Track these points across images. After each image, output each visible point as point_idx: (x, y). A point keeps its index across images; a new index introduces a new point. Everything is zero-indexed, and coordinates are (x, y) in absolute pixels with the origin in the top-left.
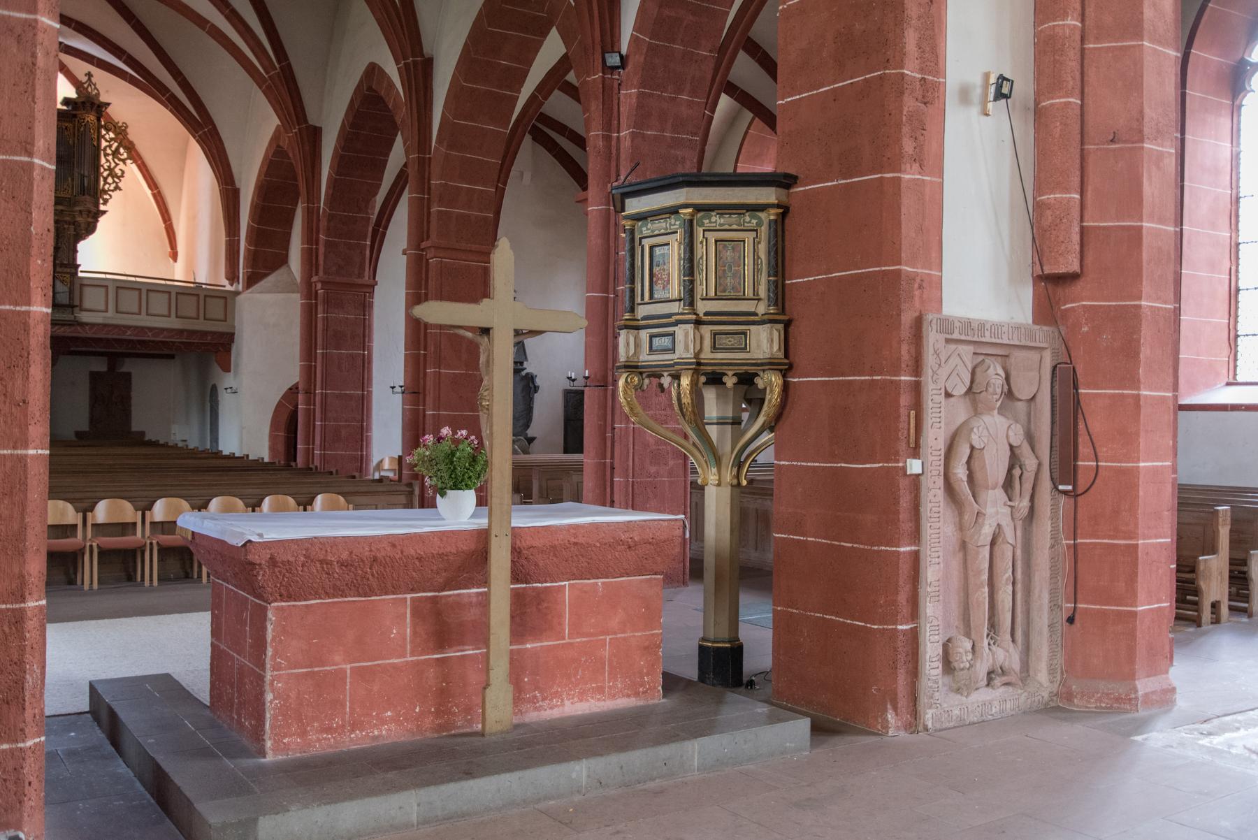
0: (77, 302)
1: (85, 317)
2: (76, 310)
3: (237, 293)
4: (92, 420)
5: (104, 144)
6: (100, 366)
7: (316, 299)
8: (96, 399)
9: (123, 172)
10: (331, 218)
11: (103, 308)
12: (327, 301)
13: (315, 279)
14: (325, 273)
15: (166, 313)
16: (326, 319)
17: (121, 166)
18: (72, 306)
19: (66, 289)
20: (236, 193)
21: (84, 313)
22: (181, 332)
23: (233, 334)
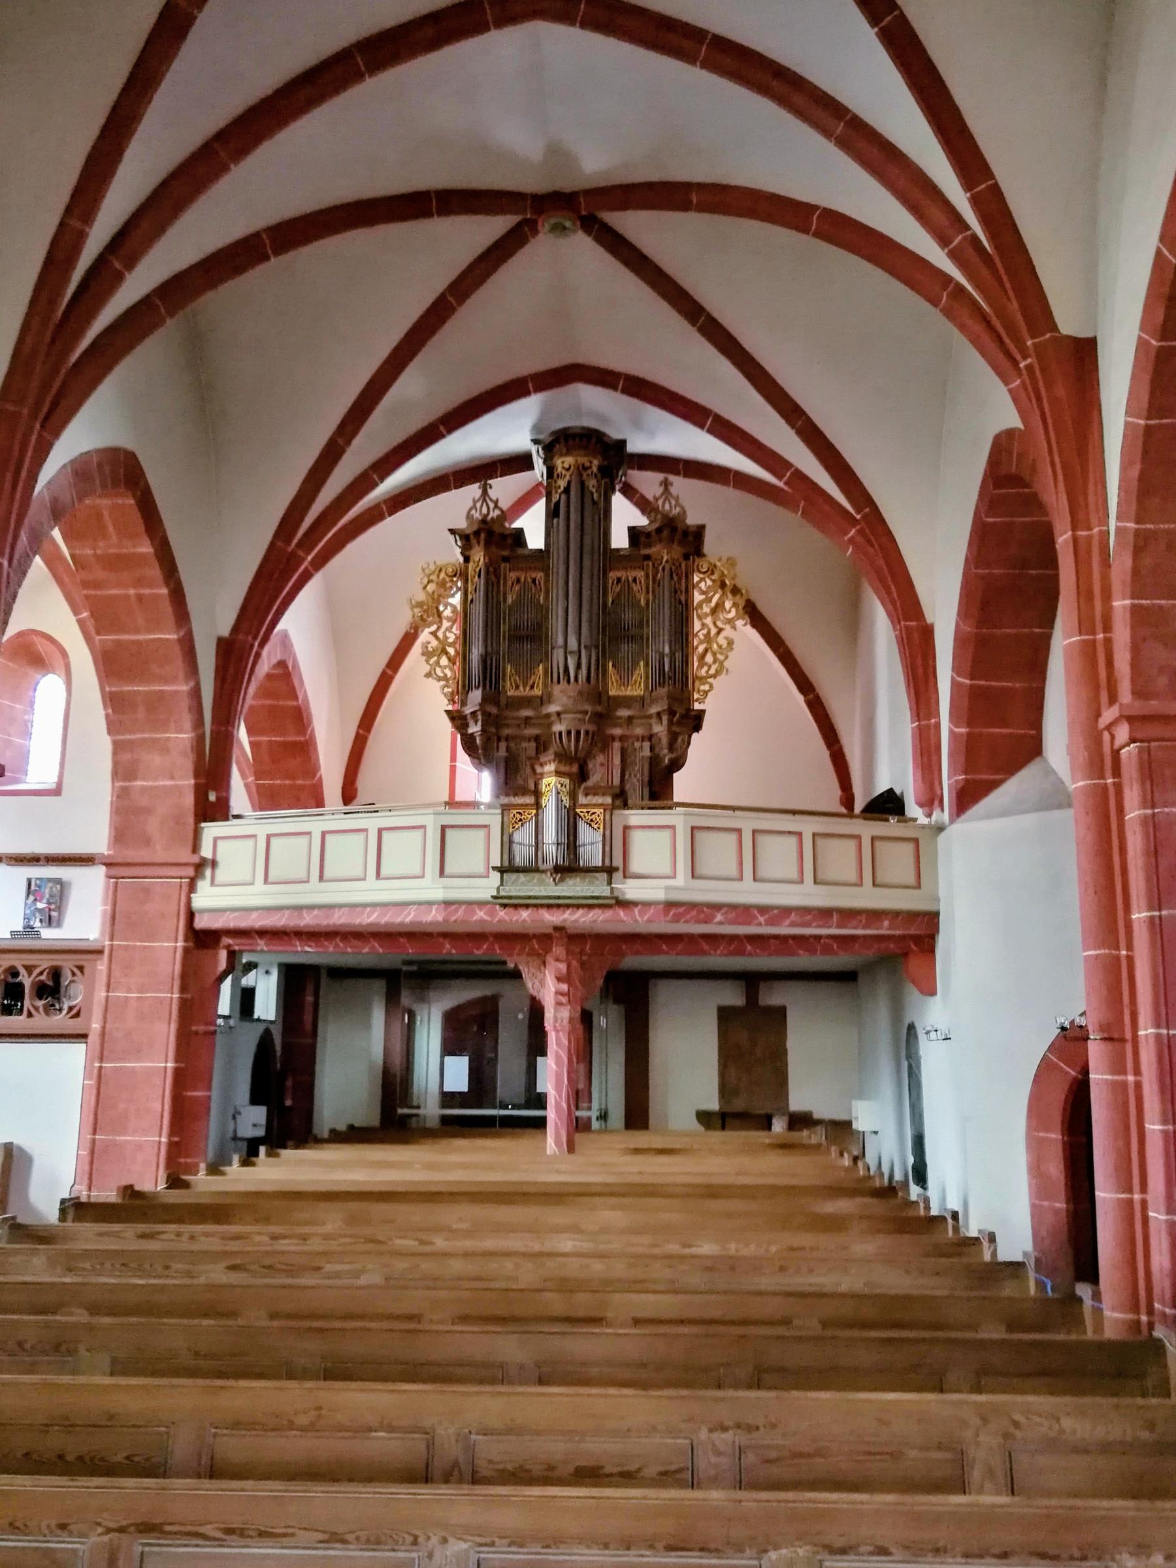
0: (618, 862)
1: (631, 890)
2: (618, 876)
3: (940, 829)
4: (725, 1091)
5: (698, 597)
6: (733, 996)
7: (1117, 771)
8: (728, 1056)
9: (730, 643)
10: (1141, 544)
11: (667, 870)
12: (1149, 772)
13: (1109, 715)
14: (1138, 693)
15: (794, 875)
16: (1151, 825)
17: (728, 631)
18: (610, 871)
19: (597, 837)
20: (927, 633)
21: (629, 881)
22: (824, 914)
23: (932, 919)
